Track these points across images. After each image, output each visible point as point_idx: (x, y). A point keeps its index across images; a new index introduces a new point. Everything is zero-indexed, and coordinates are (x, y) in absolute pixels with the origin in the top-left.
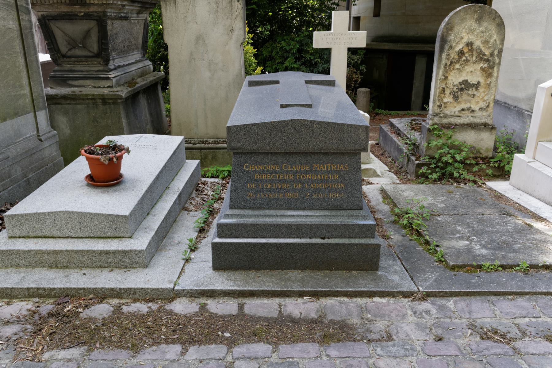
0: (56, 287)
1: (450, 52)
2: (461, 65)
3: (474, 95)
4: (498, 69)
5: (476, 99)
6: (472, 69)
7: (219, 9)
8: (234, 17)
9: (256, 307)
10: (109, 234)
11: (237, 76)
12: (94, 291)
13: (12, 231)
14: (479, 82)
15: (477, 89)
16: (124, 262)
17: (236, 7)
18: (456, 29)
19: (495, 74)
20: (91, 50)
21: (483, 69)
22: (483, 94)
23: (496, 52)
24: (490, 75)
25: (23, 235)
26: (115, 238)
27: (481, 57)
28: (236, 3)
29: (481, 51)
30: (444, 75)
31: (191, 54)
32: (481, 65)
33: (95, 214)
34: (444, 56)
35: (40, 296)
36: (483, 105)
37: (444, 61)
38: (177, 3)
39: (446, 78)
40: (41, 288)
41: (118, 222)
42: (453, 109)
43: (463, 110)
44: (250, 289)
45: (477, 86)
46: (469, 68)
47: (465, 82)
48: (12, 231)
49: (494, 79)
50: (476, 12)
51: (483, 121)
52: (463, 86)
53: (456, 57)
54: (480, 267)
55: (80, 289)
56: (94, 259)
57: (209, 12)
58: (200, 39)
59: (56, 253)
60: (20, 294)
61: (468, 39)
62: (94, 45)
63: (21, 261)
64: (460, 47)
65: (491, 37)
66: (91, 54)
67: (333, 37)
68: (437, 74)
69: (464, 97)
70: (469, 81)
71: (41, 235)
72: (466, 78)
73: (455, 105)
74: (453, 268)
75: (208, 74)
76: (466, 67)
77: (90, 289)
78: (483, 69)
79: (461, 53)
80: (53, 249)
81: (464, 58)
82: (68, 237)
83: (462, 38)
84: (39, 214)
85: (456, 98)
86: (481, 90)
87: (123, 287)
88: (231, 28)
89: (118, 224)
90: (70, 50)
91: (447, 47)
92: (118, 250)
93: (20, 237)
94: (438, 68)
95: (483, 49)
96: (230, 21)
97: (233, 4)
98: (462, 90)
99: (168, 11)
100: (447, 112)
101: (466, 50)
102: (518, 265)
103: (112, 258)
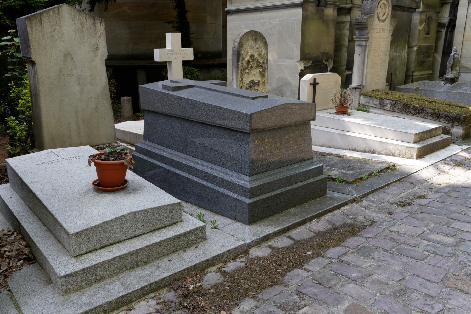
0: (165, 276)
1: (243, 61)
2: (249, 70)
3: (257, 90)
4: (267, 71)
6: (254, 73)
7: (84, 29)
8: (98, 36)
9: (300, 233)
10: (167, 223)
11: (104, 88)
12: (195, 267)
13: (80, 248)
14: (259, 81)
15: (258, 85)
16: (191, 241)
17: (99, 28)
18: (245, 46)
19: (266, 75)
21: (260, 72)
22: (261, 89)
23: (265, 61)
24: (263, 76)
25: (90, 250)
26: (171, 225)
27: (259, 65)
28: (99, 24)
29: (258, 61)
30: (241, 78)
31: (60, 71)
32: (259, 69)
33: (156, 207)
35: (153, 291)
37: (240, 68)
38: (43, 22)
39: (242, 79)
40: (153, 283)
41: (174, 209)
44: (287, 225)
45: (258, 83)
46: (253, 72)
47: (252, 81)
48: (80, 248)
49: (266, 78)
50: (253, 35)
53: (246, 65)
54: (361, 179)
55: (185, 270)
56: (169, 246)
57: (75, 31)
58: (67, 56)
59: (138, 252)
60: (135, 297)
61: (251, 53)
63: (105, 273)
64: (247, 58)
65: (262, 51)
67: (172, 52)
71: (108, 243)
72: (252, 79)
74: (352, 183)
75: (77, 88)
76: (252, 71)
77: (192, 267)
79: (248, 62)
80: (134, 249)
81: (250, 66)
82: (132, 238)
83: (248, 52)
84: (107, 222)
86: (261, 86)
87: (214, 255)
88: (96, 46)
89: (174, 211)
91: (241, 58)
92: (188, 231)
93: (86, 253)
95: (259, 59)
96: (95, 40)
97: (96, 25)
99: (34, 30)
102: (373, 173)
103: (183, 240)
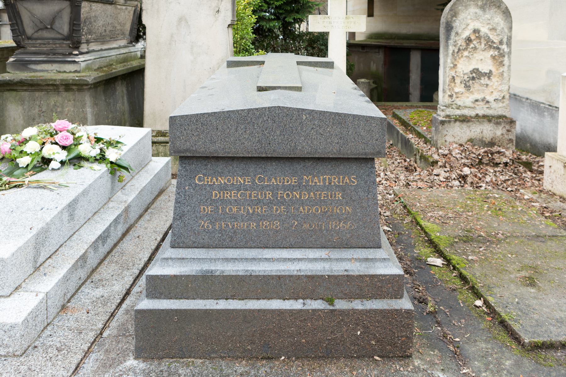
2: (470, 52)
4: (509, 57)
5: (491, 89)
6: (482, 57)
14: (491, 71)
20: (60, 31)
23: (505, 40)
27: (490, 45)
31: (172, 36)
34: (451, 42)
36: (496, 95)
37: (451, 48)
39: (455, 66)
42: (467, 99)
43: (477, 101)
45: (489, 75)
46: (479, 55)
51: (500, 112)
52: (474, 75)
53: (464, 44)
62: (64, 27)
64: (466, 34)
66: (60, 36)
69: (476, 86)
70: (480, 70)
72: (476, 67)
73: (467, 95)
76: (475, 55)
78: (493, 57)
79: (469, 40)
81: (472, 46)
85: (467, 87)
90: (37, 32)
94: (447, 55)
95: (491, 37)
98: (473, 78)
100: (459, 102)
101: (473, 37)
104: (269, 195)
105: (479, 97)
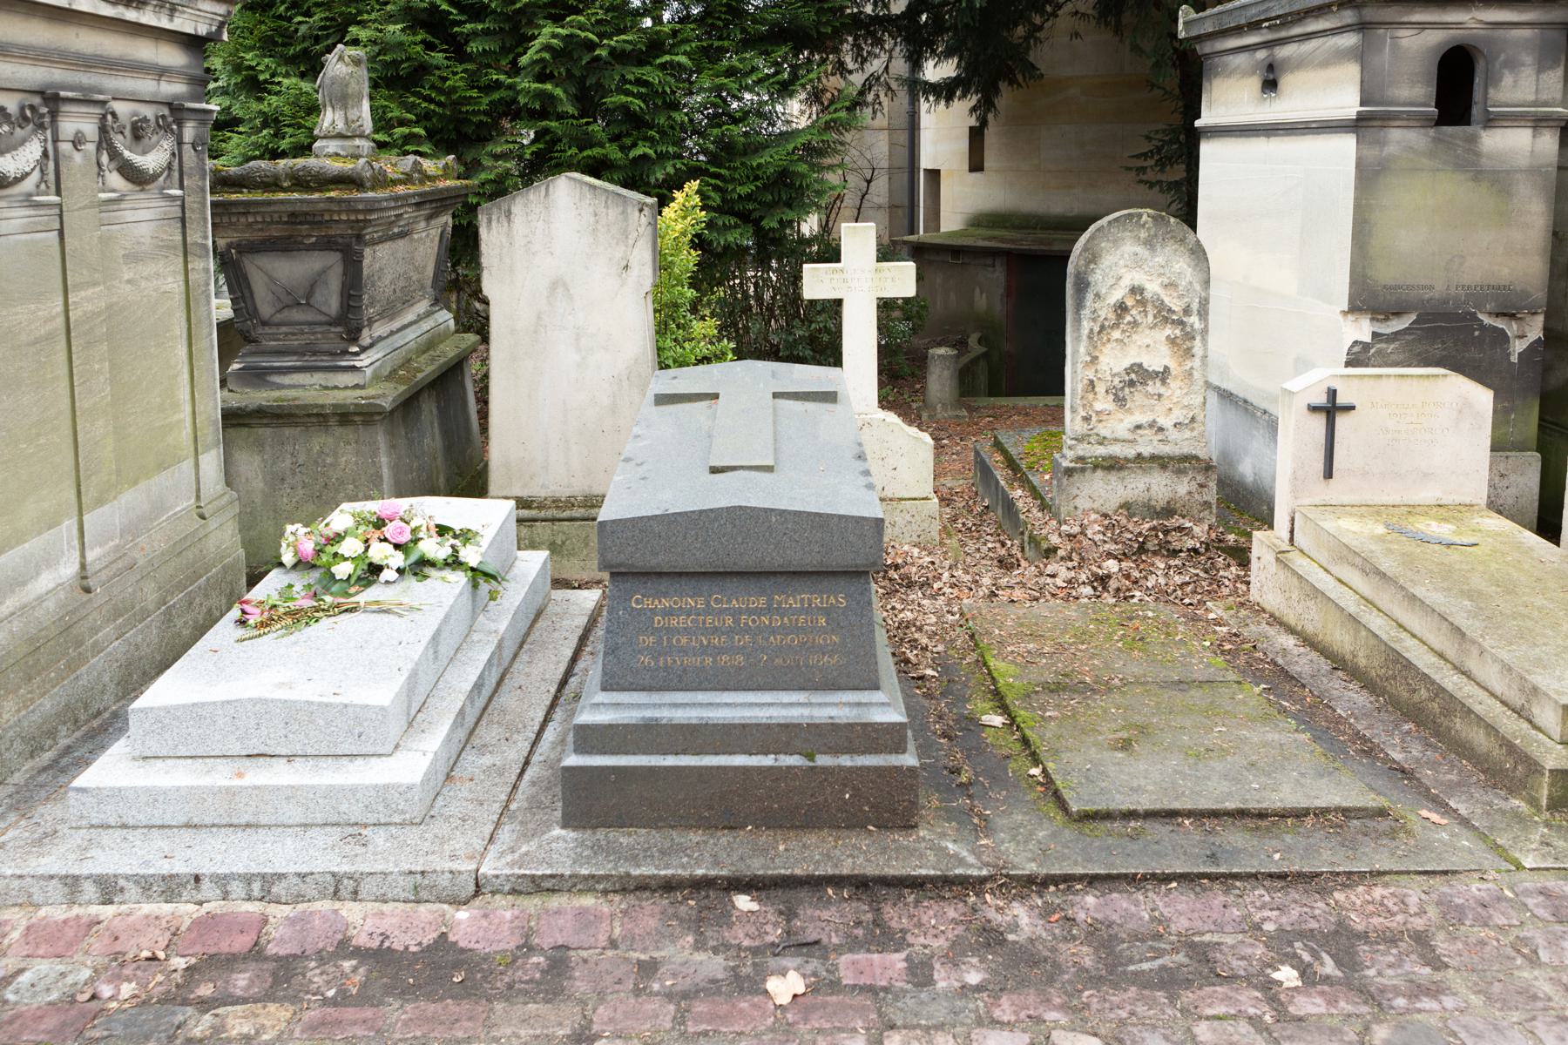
5: (1166, 404)
6: (1148, 341)
14: (1166, 368)
15: (1163, 381)
20: (324, 309)
23: (1195, 306)
27: (1164, 316)
34: (1086, 312)
36: (1178, 415)
37: (1086, 325)
39: (1094, 359)
42: (1118, 425)
43: (1139, 427)
45: (1164, 375)
46: (1143, 337)
47: (1137, 368)
51: (1186, 449)
52: (1133, 376)
53: (1112, 316)
62: (331, 301)
64: (1117, 295)
66: (323, 318)
68: (1075, 352)
69: (1137, 398)
70: (1145, 366)
72: (1138, 361)
73: (1120, 415)
76: (1135, 337)
78: (1172, 341)
79: (1121, 308)
81: (1128, 318)
85: (1120, 401)
91: (1090, 296)
94: (1078, 339)
95: (1167, 300)
98: (1132, 383)
99: (494, 231)
100: (1103, 430)
101: (1130, 302)
104: (729, 621)
105: (1143, 419)
